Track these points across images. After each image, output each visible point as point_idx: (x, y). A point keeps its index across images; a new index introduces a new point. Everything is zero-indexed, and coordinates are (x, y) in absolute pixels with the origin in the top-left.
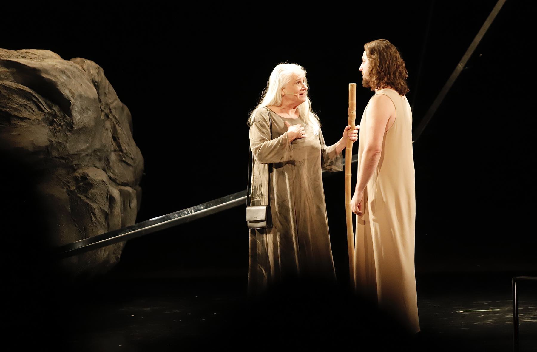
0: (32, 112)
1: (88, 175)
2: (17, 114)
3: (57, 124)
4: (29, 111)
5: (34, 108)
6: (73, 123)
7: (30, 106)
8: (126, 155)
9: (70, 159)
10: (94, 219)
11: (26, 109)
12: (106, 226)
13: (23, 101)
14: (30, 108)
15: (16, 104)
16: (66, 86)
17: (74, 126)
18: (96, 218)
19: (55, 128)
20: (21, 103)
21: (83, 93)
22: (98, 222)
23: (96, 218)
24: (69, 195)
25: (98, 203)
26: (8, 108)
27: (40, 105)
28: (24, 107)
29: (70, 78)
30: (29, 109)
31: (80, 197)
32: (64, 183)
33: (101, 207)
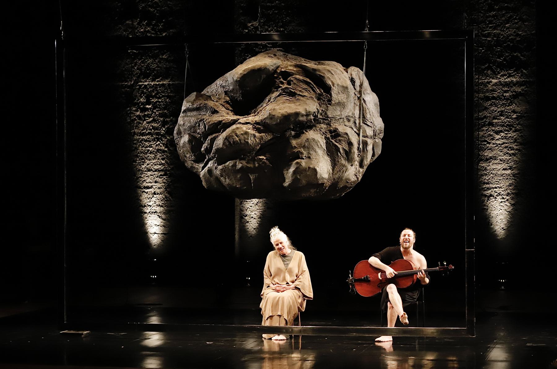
0: (309, 93)
1: (337, 129)
2: (301, 93)
3: (323, 100)
4: (308, 92)
5: (311, 91)
6: (332, 100)
7: (309, 89)
8: (368, 120)
9: (329, 120)
10: (339, 154)
11: (306, 91)
12: (347, 158)
13: (305, 86)
14: (309, 90)
15: (301, 88)
16: (329, 79)
17: (332, 101)
18: (341, 154)
19: (321, 102)
20: (304, 88)
21: (340, 83)
22: (342, 155)
23: (341, 154)
24: (326, 140)
25: (341, 145)
26: (296, 90)
27: (315, 89)
28: (305, 90)
29: (333, 75)
30: (308, 91)
31: (332, 141)
32: (323, 133)
33: (344, 147)
